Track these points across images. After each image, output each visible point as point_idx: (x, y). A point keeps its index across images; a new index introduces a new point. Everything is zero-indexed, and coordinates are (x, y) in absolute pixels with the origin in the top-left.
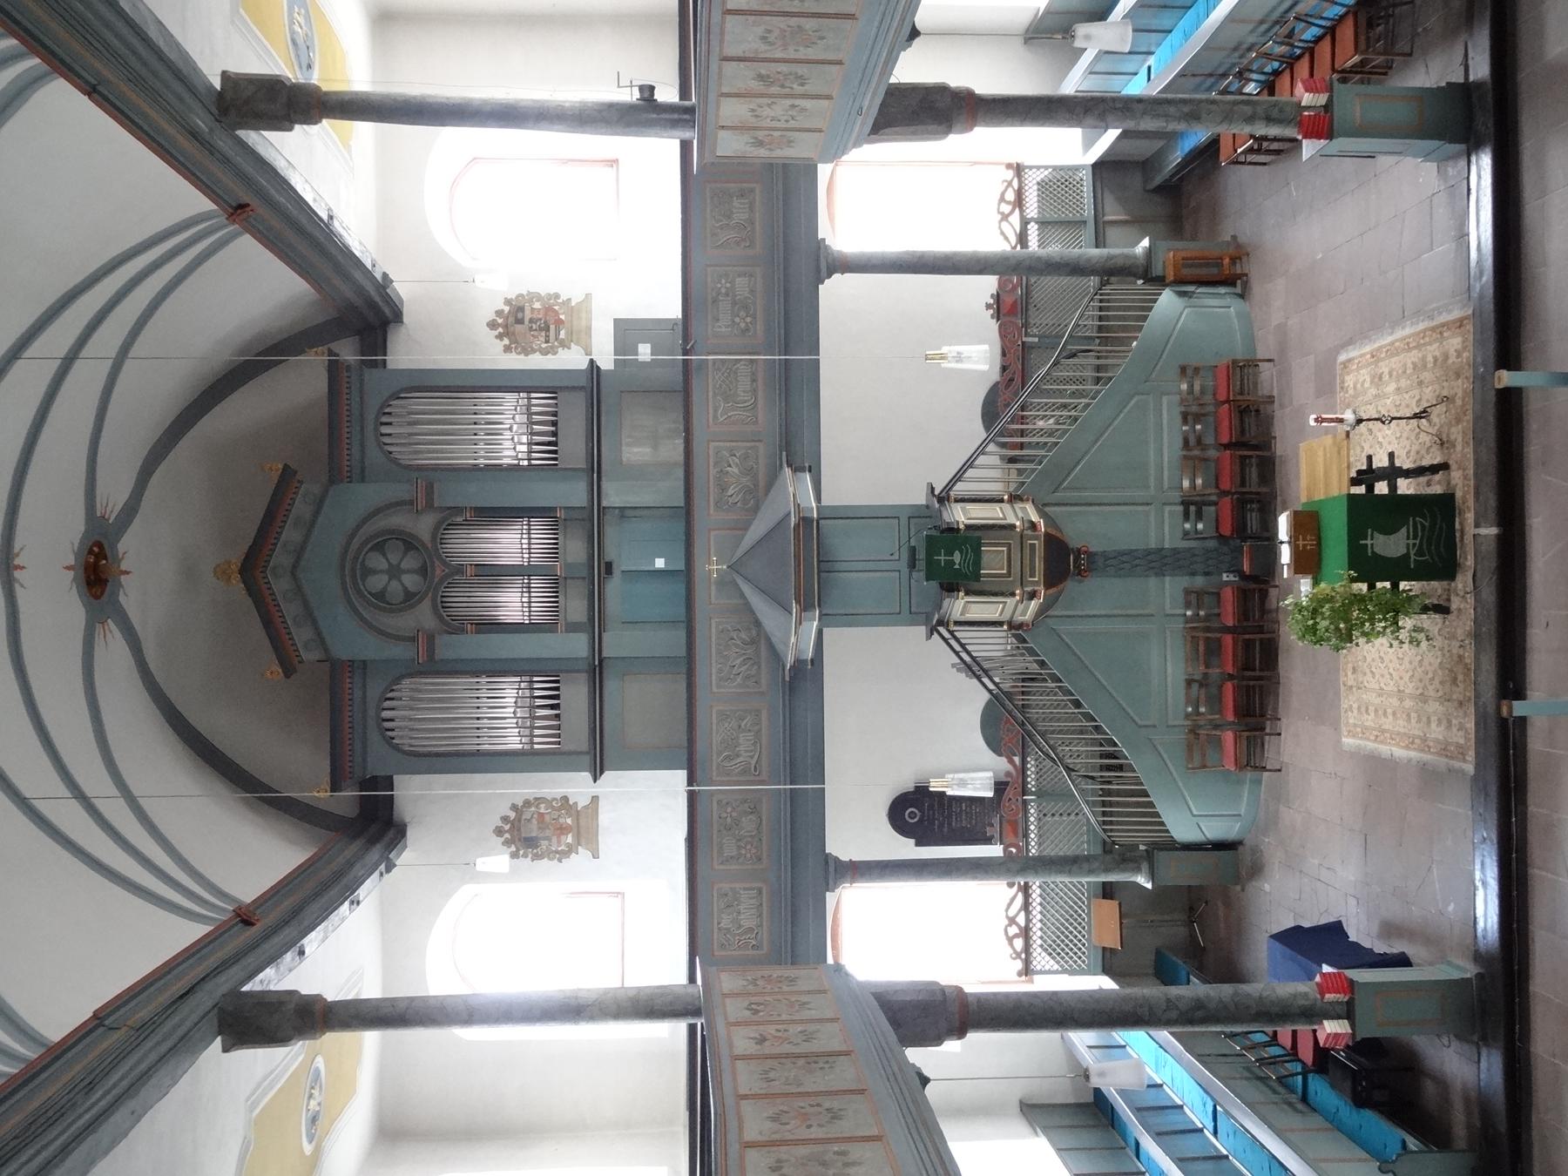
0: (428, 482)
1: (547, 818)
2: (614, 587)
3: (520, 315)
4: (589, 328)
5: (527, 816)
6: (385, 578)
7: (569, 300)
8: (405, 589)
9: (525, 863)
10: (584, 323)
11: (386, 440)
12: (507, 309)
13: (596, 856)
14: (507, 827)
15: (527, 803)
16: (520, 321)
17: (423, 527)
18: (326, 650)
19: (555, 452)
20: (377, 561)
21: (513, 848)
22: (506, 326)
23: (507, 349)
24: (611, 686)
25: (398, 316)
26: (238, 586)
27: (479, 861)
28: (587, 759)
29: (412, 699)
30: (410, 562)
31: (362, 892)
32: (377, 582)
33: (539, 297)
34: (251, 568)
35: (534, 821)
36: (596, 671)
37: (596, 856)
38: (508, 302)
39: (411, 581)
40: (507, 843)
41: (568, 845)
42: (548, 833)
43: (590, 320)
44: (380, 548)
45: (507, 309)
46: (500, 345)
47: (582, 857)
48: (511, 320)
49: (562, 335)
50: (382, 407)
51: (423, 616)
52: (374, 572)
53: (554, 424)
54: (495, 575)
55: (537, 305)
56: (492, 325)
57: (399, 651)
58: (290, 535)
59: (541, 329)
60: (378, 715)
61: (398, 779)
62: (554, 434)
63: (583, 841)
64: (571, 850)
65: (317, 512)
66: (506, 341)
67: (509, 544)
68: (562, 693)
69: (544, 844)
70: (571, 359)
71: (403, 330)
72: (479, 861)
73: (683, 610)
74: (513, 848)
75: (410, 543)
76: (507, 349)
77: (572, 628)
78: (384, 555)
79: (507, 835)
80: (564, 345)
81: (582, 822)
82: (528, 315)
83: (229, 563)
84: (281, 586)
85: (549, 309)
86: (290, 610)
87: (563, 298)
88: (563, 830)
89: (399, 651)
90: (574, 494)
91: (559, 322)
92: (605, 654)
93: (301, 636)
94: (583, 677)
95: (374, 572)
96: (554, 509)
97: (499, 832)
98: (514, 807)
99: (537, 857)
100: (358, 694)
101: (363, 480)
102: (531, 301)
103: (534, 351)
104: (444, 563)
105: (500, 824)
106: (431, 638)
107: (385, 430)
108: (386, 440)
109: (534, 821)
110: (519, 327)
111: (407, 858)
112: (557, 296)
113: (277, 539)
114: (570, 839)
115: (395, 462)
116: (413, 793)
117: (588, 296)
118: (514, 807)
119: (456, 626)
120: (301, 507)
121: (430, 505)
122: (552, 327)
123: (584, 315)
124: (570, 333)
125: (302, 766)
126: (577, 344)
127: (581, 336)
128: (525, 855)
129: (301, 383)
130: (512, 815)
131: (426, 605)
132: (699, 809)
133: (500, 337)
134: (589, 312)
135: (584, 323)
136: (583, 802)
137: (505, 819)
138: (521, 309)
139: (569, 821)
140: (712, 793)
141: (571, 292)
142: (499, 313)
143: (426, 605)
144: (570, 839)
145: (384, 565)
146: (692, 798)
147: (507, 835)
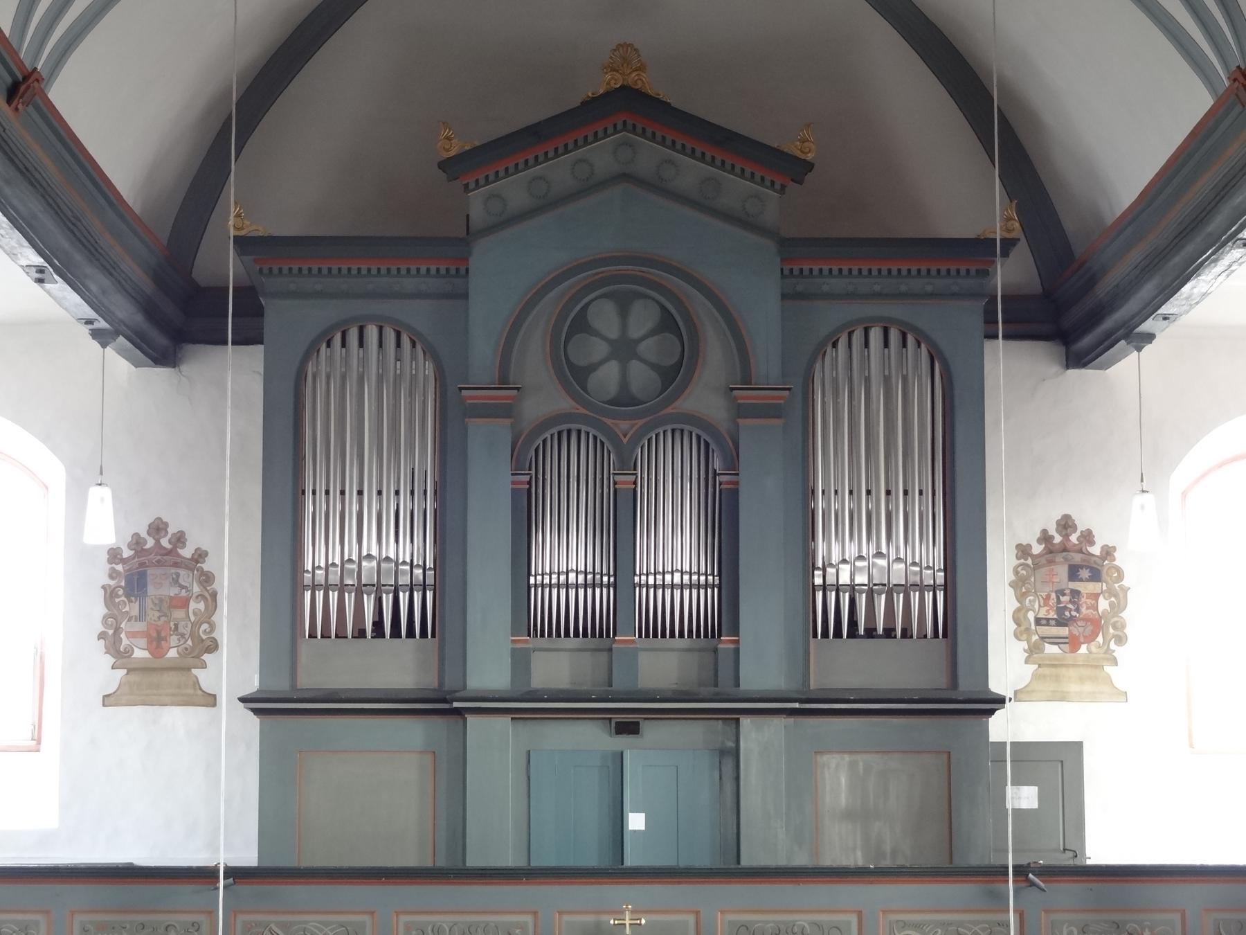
0: (786, 409)
1: (178, 614)
2: (592, 738)
3: (1085, 573)
4: (1063, 697)
5: (185, 576)
6: (614, 334)
7: (1115, 662)
8: (593, 368)
9: (100, 574)
10: (1074, 688)
11: (858, 337)
12: (1096, 550)
13: (108, 700)
14: (165, 542)
15: (207, 579)
16: (1073, 573)
17: (705, 398)
18: (490, 230)
19: (838, 634)
20: (643, 318)
21: (127, 553)
22: (1064, 549)
23: (1023, 551)
24: (413, 731)
25: (1077, 360)
26: (600, 84)
27: (106, 492)
28: (281, 685)
29: (398, 379)
30: (641, 377)
31: (59, 287)
32: (605, 317)
33: (1119, 607)
34: (629, 105)
35: (174, 591)
36: (443, 704)
37: (108, 700)
38: (1108, 552)
39: (608, 377)
40: (137, 542)
41: (129, 652)
42: (153, 615)
43: (1080, 698)
44: (667, 324)
45: (1096, 550)
46: (1030, 537)
47: (107, 676)
48: (1077, 558)
49: (1052, 649)
50: (915, 330)
51: (544, 399)
52: (624, 312)
53: (889, 633)
54: (618, 526)
55: (1103, 604)
56: (1066, 524)
57: (483, 352)
58: (690, 172)
59: (1061, 610)
60: (372, 318)
61: (254, 356)
62: (870, 633)
63: (134, 678)
64: (119, 654)
65: (728, 217)
66: (1037, 549)
67: (673, 553)
68: (404, 643)
69: (134, 609)
70: (1006, 664)
71: (1055, 368)
72: (106, 492)
73: (551, 861)
74: (127, 553)
75: (674, 376)
76: (1023, 551)
77: (521, 661)
78: (652, 333)
79: (150, 543)
80: (1033, 652)
81: (169, 678)
82: (1086, 588)
83: (641, 68)
84: (602, 155)
85: (1096, 625)
86: (559, 171)
87: (1119, 651)
88: (156, 642)
89: (483, 352)
90: (763, 663)
91: (1073, 643)
92: (471, 720)
93: (514, 190)
94: (430, 681)
95: (624, 312)
96: (735, 630)
97: (158, 528)
98: (200, 555)
99: (110, 595)
100: (409, 284)
101: (784, 296)
102: (1111, 593)
103: (1021, 597)
104: (636, 440)
105: (172, 530)
106: (505, 411)
107: (875, 335)
108: (858, 337)
109: (174, 591)
110: (1062, 571)
111: (118, 366)
112: (1121, 640)
113: (683, 151)
114: (140, 654)
115: (819, 352)
116: (232, 379)
117: (1123, 695)
118: (200, 555)
119: (527, 456)
120: (737, 189)
121: (741, 412)
122: (1064, 631)
123: (1088, 687)
124: (1055, 663)
125: (286, 187)
126: (1035, 676)
127: (1048, 683)
128: (113, 575)
129: (959, 195)
130: (187, 552)
131: (565, 404)
132: (186, 890)
133: (1045, 538)
134: (1093, 698)
135: (1074, 688)
137: (180, 539)
138: (1096, 576)
139: (172, 653)
140: (212, 913)
141: (1131, 663)
142: (1088, 537)
143: (565, 404)
144: (140, 654)
145: (635, 332)
146: (203, 876)
147: (150, 543)
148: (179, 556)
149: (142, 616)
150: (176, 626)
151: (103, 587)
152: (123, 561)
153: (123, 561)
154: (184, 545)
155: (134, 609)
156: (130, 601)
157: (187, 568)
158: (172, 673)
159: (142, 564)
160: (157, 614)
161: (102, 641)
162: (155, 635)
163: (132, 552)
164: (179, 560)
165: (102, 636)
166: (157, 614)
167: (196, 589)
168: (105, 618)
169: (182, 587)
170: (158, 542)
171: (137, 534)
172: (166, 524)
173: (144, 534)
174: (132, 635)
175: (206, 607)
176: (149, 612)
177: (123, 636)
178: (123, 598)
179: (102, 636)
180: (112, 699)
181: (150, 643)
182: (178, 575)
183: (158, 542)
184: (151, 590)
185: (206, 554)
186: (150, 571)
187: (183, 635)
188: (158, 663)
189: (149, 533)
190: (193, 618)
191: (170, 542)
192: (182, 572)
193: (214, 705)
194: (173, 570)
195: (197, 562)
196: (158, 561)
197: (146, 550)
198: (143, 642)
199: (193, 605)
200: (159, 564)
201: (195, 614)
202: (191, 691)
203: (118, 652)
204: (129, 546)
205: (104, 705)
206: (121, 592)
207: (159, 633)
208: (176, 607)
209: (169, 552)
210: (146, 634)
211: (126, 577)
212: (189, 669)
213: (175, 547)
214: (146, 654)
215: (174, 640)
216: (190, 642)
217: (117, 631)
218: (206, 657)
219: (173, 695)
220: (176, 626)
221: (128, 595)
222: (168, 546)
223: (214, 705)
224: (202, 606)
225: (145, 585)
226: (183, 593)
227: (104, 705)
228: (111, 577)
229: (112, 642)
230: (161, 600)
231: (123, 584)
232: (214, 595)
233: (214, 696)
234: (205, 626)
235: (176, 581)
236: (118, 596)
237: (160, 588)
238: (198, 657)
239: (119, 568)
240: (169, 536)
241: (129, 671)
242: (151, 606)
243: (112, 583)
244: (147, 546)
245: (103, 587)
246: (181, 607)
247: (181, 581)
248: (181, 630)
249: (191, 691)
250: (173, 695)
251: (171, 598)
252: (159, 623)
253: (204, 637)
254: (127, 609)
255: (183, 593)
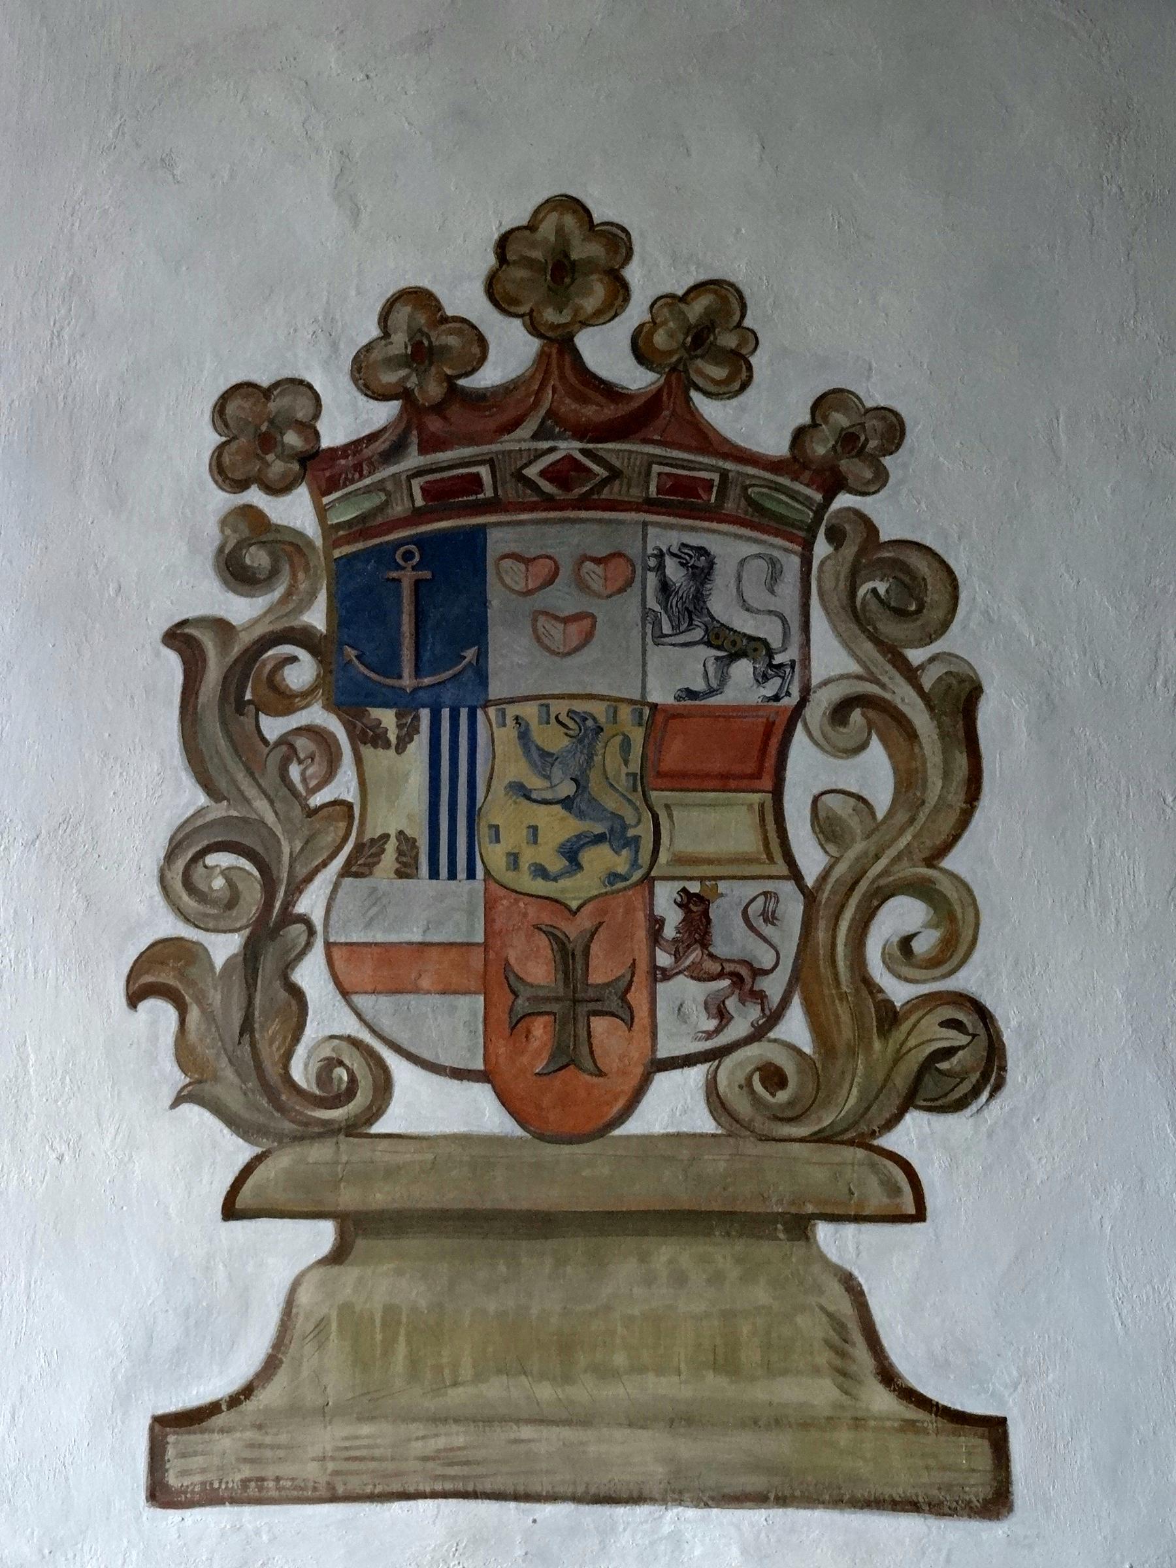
1: (714, 826)
5: (746, 577)
14: (607, 352)
15: (907, 591)
35: (675, 673)
37: (185, 1458)
40: (418, 346)
42: (524, 832)
63: (387, 1282)
69: (397, 790)
74: (347, 417)
79: (510, 352)
81: (643, 1283)
88: (556, 1027)
97: (559, 261)
98: (852, 441)
99: (220, 692)
105: (650, 277)
109: (675, 673)
114: (430, 1106)
118: (852, 441)
130: (759, 420)
136: (934, 1293)
137: (710, 333)
139: (674, 1105)
144: (430, 1106)
148: (705, 439)
149: (448, 841)
150: (696, 907)
151: (179, 637)
152: (321, 468)
153: (321, 468)
154: (738, 376)
155: (397, 790)
156: (367, 736)
157: (759, 518)
158: (666, 1253)
159: (447, 493)
160: (557, 827)
161: (160, 1015)
162: (539, 971)
163: (382, 413)
164: (707, 468)
165: (157, 976)
166: (557, 827)
167: (832, 658)
168: (186, 850)
169: (732, 646)
170: (559, 348)
171: (419, 298)
172: (618, 242)
173: (465, 299)
174: (373, 969)
175: (908, 781)
176: (499, 809)
177: (311, 974)
178: (317, 715)
179: (157, 976)
180: (221, 1445)
181: (508, 1021)
182: (701, 567)
183: (559, 348)
184: (514, 661)
185: (893, 429)
186: (502, 538)
187: (744, 979)
188: (570, 1177)
189: (497, 293)
190: (811, 858)
191: (642, 349)
192: (729, 548)
193: (997, 1501)
194: (667, 535)
195: (834, 484)
196: (564, 473)
197: (479, 400)
198: (455, 1023)
199: (808, 768)
200: (570, 490)
201: (827, 829)
202: (821, 1393)
203: (276, 1088)
204: (365, 375)
205: (160, 1494)
206: (302, 672)
207: (569, 957)
208: (684, 780)
209: (636, 418)
210: (487, 971)
211: (343, 571)
212: (799, 1227)
213: (679, 381)
214: (478, 1111)
215: (681, 1009)
216: (795, 1028)
217: (272, 935)
218: (915, 1135)
219: (683, 1420)
220: (696, 907)
221: (350, 701)
222: (638, 379)
223: (997, 1501)
224: (873, 773)
225: (475, 631)
226: (743, 685)
227: (160, 1494)
228: (235, 572)
229: (227, 1015)
230: (587, 733)
231: (316, 618)
232: (960, 701)
233: (994, 1429)
234: (902, 916)
235: (685, 605)
236: (285, 701)
237: (569, 649)
238: (861, 1134)
239: (296, 511)
240: (636, 313)
241: (356, 1231)
242: (514, 768)
243: (243, 610)
244: (489, 377)
245: (179, 637)
246: (725, 781)
247: (721, 605)
248: (731, 938)
249: (821, 1393)
250: (683, 1420)
251: (656, 719)
252: (576, 888)
253: (899, 992)
254: (344, 786)
255: (743, 685)
